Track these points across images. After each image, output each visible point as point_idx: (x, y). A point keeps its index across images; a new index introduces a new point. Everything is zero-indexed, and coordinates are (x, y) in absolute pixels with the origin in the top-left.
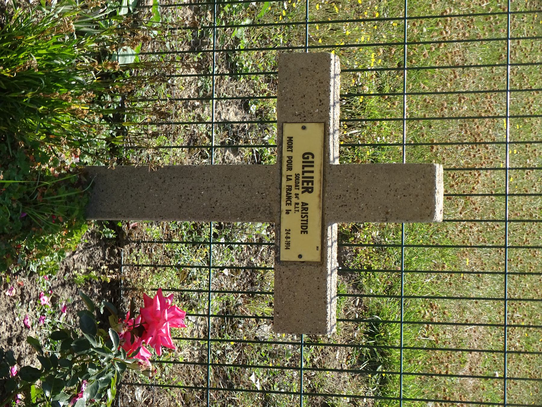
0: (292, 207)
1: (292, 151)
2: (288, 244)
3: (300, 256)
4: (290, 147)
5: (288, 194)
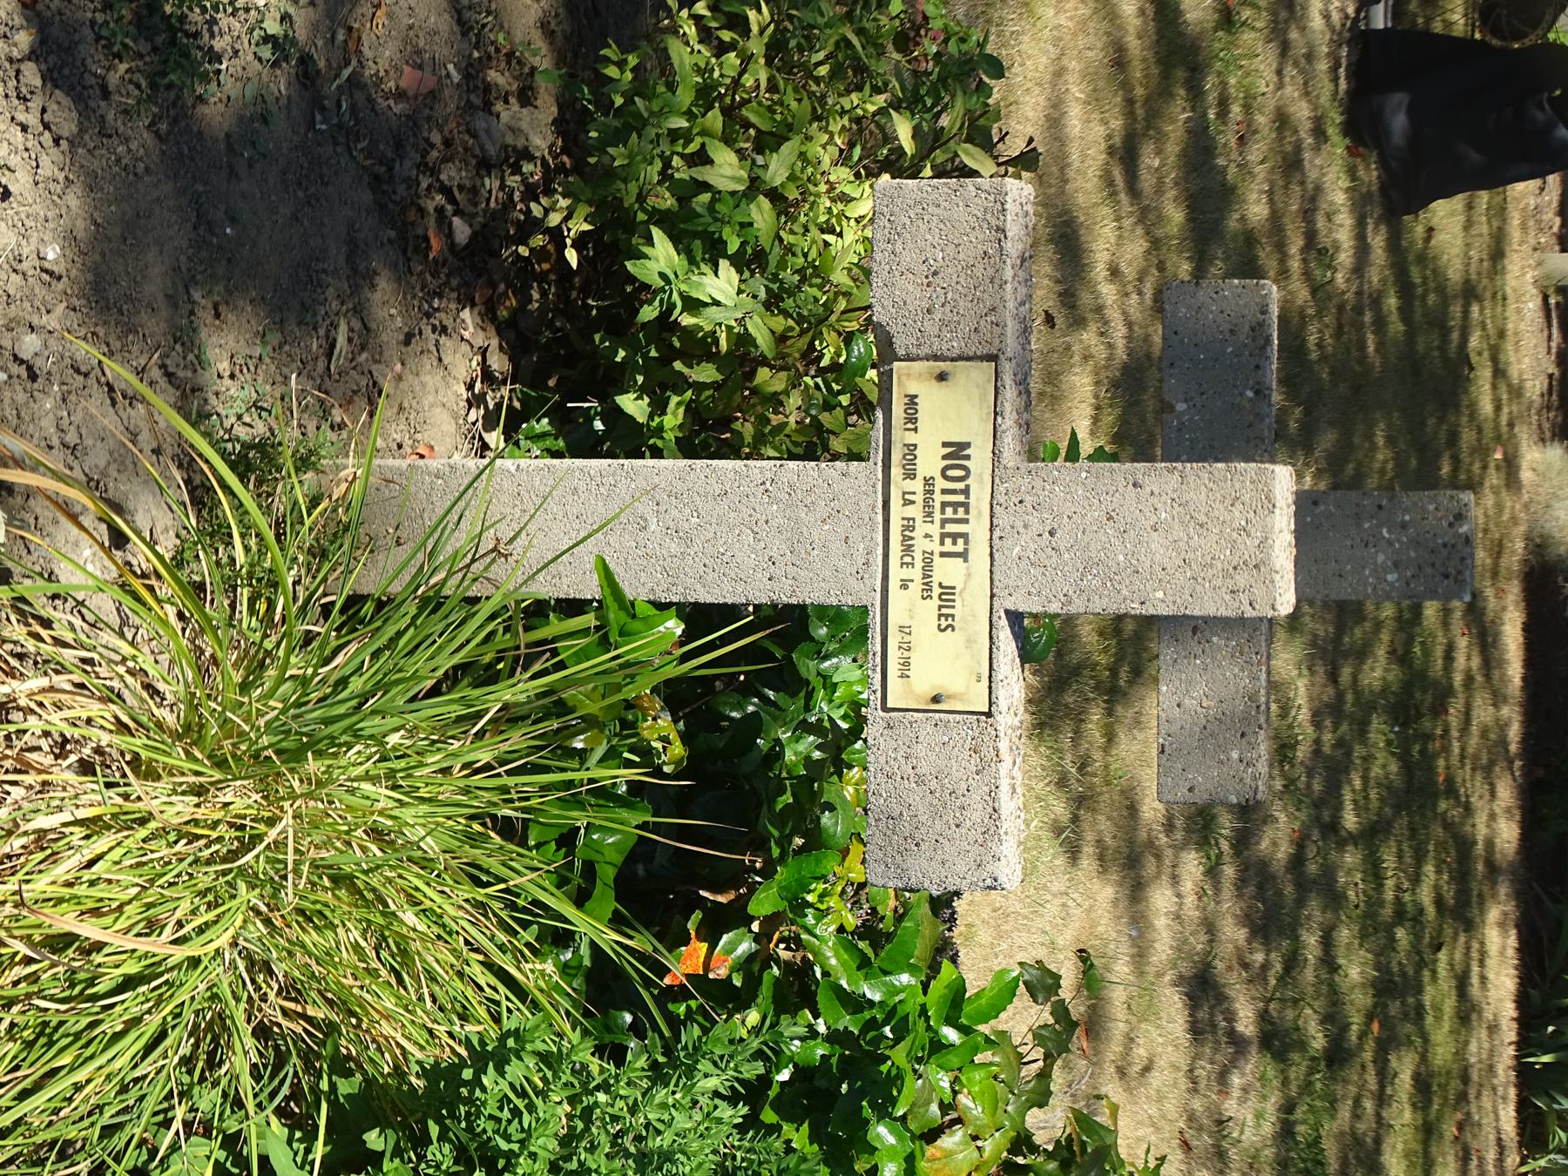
0: (916, 573)
1: (915, 430)
2: (906, 664)
3: (936, 699)
4: (912, 419)
5: (905, 538)
